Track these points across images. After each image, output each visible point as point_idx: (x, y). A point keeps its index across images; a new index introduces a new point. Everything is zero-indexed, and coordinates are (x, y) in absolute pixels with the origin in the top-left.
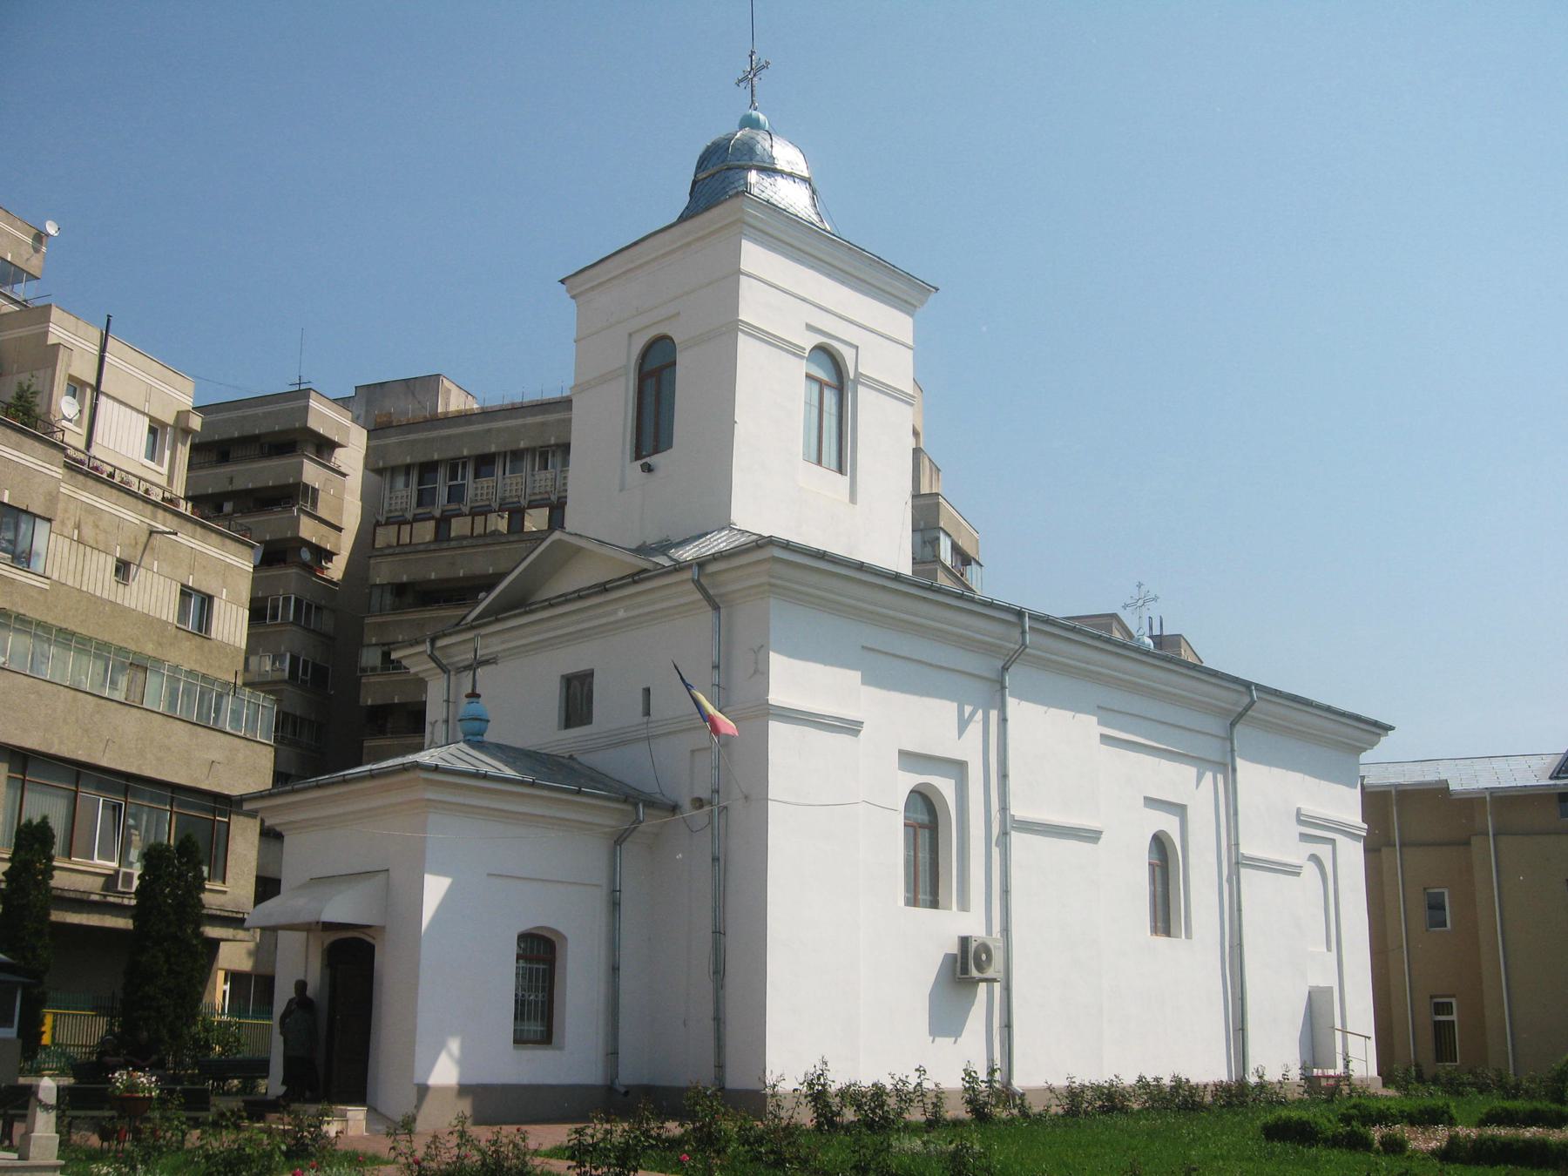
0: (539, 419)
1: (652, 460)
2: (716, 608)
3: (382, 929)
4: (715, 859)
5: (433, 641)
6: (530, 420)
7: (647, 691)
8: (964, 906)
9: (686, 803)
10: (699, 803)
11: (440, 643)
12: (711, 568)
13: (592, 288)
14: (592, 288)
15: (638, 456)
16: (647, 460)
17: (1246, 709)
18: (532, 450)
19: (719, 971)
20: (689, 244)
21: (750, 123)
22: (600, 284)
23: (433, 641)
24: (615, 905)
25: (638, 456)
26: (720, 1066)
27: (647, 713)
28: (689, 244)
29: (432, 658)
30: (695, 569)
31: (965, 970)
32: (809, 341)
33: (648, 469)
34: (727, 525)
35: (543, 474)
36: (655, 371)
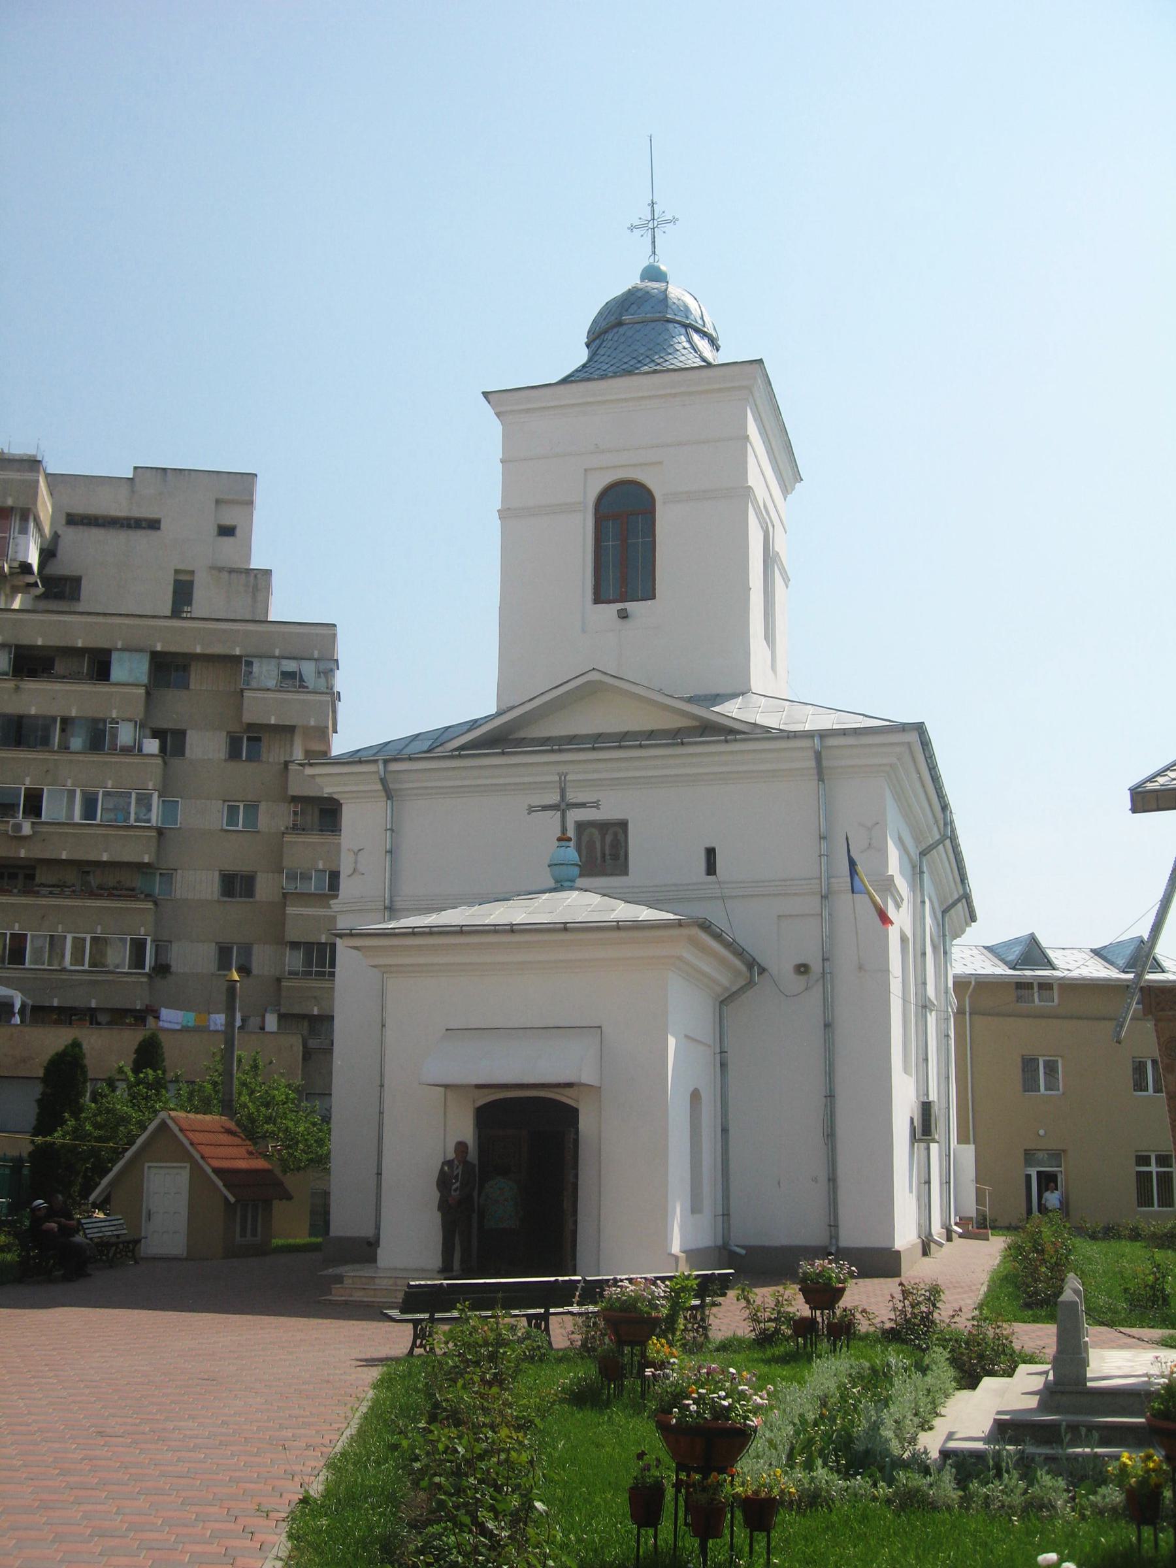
2: (821, 779)
3: (594, 1090)
4: (827, 1026)
7: (711, 853)
9: (781, 965)
10: (802, 969)
11: (394, 767)
12: (831, 742)
13: (527, 411)
14: (527, 411)
15: (598, 600)
16: (620, 606)
19: (830, 1135)
20: (674, 395)
21: (653, 274)
23: (386, 762)
24: (723, 1065)
25: (598, 600)
26: (834, 1226)
27: (711, 869)
28: (674, 395)
29: (383, 781)
30: (817, 740)
33: (623, 615)
34: (744, 692)
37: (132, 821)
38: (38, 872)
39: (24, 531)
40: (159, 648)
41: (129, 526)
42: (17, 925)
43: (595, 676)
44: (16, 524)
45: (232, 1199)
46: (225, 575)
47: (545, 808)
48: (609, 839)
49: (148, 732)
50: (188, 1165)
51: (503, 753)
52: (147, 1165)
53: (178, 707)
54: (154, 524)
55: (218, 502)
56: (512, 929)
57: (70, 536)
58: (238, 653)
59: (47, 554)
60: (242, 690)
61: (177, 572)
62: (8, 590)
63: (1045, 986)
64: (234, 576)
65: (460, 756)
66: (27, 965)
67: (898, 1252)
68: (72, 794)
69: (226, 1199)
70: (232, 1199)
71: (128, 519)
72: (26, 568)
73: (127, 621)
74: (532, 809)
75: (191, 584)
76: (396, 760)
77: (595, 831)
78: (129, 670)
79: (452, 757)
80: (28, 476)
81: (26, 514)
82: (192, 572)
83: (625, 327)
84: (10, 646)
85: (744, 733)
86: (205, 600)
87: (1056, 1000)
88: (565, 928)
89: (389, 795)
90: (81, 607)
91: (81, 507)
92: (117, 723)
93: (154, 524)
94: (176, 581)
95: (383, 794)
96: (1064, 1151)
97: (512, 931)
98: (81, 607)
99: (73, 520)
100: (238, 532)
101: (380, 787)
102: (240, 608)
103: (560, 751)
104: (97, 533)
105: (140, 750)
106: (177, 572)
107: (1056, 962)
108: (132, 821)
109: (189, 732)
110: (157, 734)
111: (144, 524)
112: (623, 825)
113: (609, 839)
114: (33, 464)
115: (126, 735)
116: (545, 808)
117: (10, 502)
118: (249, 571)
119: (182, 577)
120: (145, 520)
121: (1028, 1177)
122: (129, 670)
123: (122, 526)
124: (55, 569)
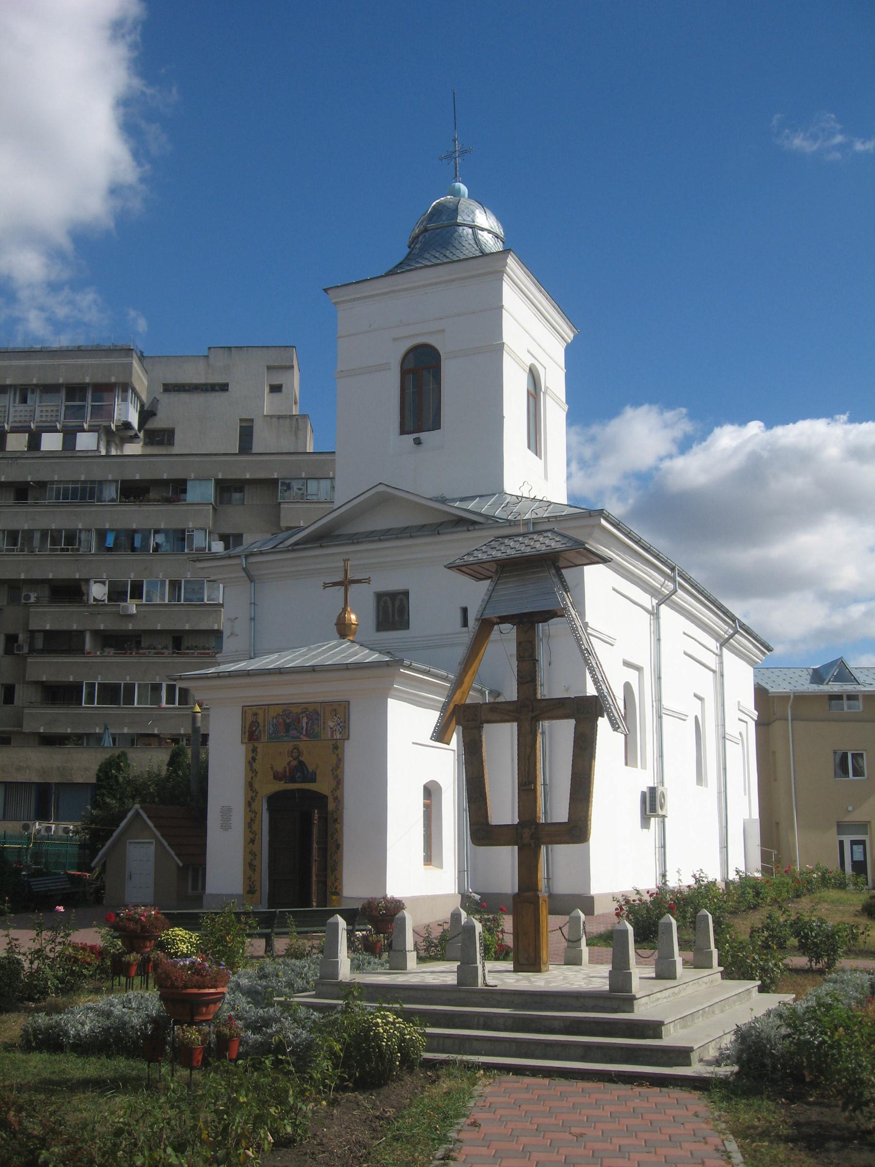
0: (23, 363)
1: (423, 435)
5: (246, 556)
6: (15, 363)
8: (644, 767)
13: (354, 300)
14: (354, 300)
15: (403, 432)
16: (416, 435)
17: (731, 636)
18: (14, 387)
20: (453, 281)
22: (365, 297)
23: (246, 556)
25: (403, 432)
28: (453, 281)
31: (653, 809)
32: (529, 361)
33: (418, 442)
34: (502, 492)
35: (22, 407)
36: (421, 370)
37: (206, 601)
38: (143, 639)
39: (124, 400)
40: (220, 477)
41: (207, 390)
42: (99, 677)
43: (381, 488)
44: (118, 392)
45: (181, 864)
46: (275, 420)
47: (335, 584)
48: (397, 603)
49: (217, 536)
50: (154, 841)
51: (321, 547)
52: (128, 841)
53: (237, 517)
54: (224, 387)
55: (269, 368)
56: (280, 671)
57: (166, 400)
58: (276, 477)
59: (146, 415)
60: (280, 503)
61: (241, 420)
62: (117, 441)
63: (852, 697)
64: (281, 421)
65: (293, 550)
66: (136, 705)
67: (592, 898)
68: (163, 583)
69: (178, 865)
70: (181, 864)
71: (205, 385)
72: (127, 425)
73: (197, 459)
74: (326, 586)
75: (251, 428)
76: (252, 554)
77: (388, 599)
78: (201, 493)
79: (288, 551)
80: (125, 360)
81: (126, 387)
82: (252, 420)
83: (429, 232)
84: (117, 481)
85: (481, 523)
86: (262, 440)
87: (861, 708)
88: (313, 669)
89: (251, 579)
90: (176, 450)
91: (171, 380)
92: (193, 531)
93: (224, 387)
94: (241, 427)
95: (247, 579)
96: (869, 822)
97: (281, 673)
98: (176, 450)
99: (168, 388)
100: (284, 389)
101: (244, 574)
102: (286, 444)
103: (358, 543)
104: (184, 397)
105: (210, 549)
106: (241, 420)
107: (861, 680)
108: (206, 601)
109: (244, 535)
110: (224, 538)
111: (217, 388)
112: (406, 594)
113: (397, 603)
114: (128, 351)
115: (199, 540)
116: (335, 584)
117: (113, 380)
118: (291, 417)
119: (243, 424)
120: (218, 384)
121: (841, 843)
122: (201, 493)
123: (202, 390)
124: (154, 424)
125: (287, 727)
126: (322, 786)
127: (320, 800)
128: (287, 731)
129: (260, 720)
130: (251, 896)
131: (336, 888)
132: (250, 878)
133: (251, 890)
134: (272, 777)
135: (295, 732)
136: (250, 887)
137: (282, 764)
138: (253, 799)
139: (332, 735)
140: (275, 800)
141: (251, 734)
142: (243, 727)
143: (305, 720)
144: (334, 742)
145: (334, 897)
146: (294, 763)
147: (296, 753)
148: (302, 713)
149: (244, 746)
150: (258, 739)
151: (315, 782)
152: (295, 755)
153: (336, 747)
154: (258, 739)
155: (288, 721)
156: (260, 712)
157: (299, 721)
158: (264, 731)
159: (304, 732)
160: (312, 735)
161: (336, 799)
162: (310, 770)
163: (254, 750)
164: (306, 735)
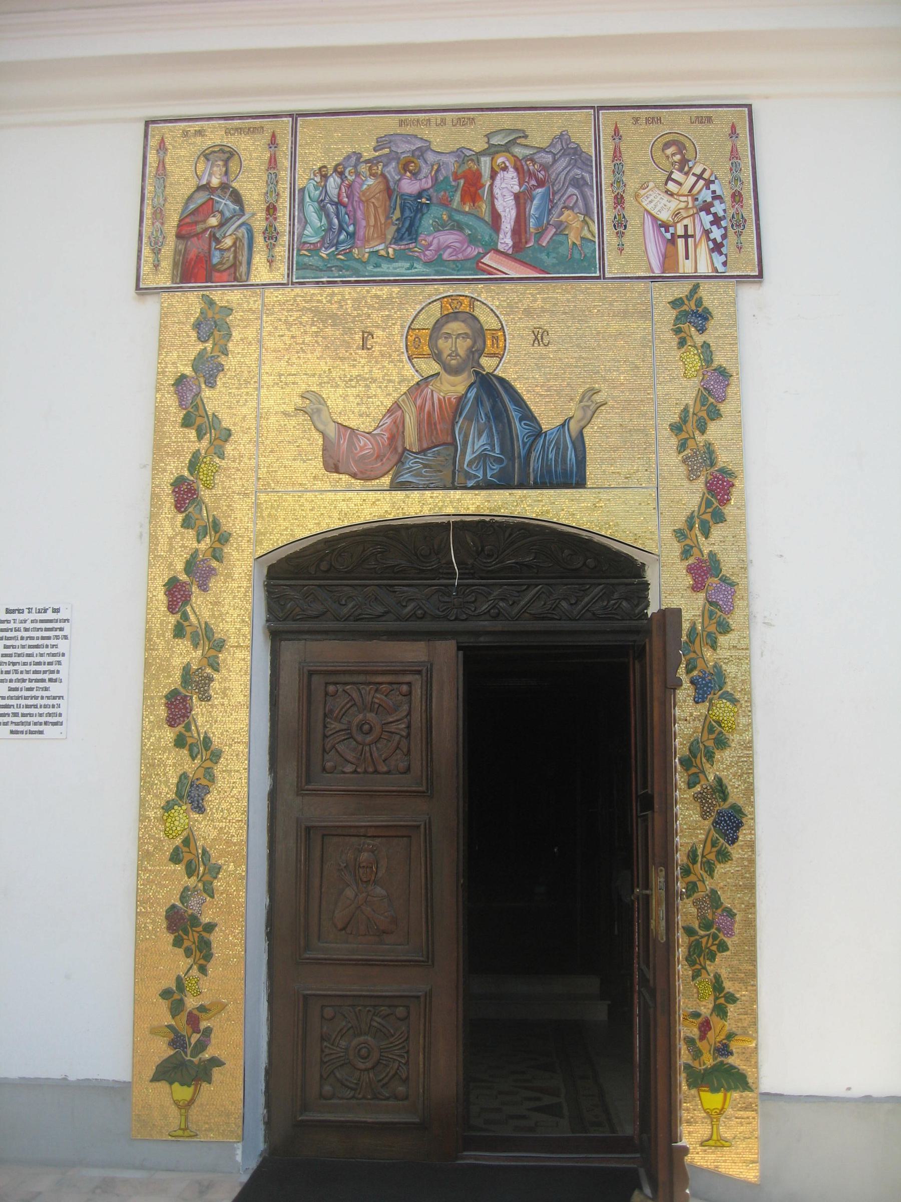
125: (408, 218)
126: (620, 504)
127: (612, 570)
128: (408, 231)
129: (252, 191)
130: (183, 1092)
131: (724, 1050)
132: (174, 997)
133: (184, 1063)
134: (317, 465)
135: (449, 238)
136: (178, 1041)
137: (372, 388)
138: (200, 571)
139: (669, 259)
140: (315, 585)
141: (199, 250)
142: (150, 210)
143: (507, 185)
144: (681, 290)
145: (713, 1100)
146: (454, 386)
147: (458, 343)
148: (492, 151)
149: (152, 306)
150: (235, 273)
151: (581, 483)
152: (455, 344)
153: (693, 316)
154: (235, 273)
155: (409, 186)
156: (252, 150)
157: (472, 186)
158: (271, 235)
159: (506, 241)
160: (553, 255)
161: (704, 571)
162: (548, 421)
163: (212, 326)
164: (518, 253)
